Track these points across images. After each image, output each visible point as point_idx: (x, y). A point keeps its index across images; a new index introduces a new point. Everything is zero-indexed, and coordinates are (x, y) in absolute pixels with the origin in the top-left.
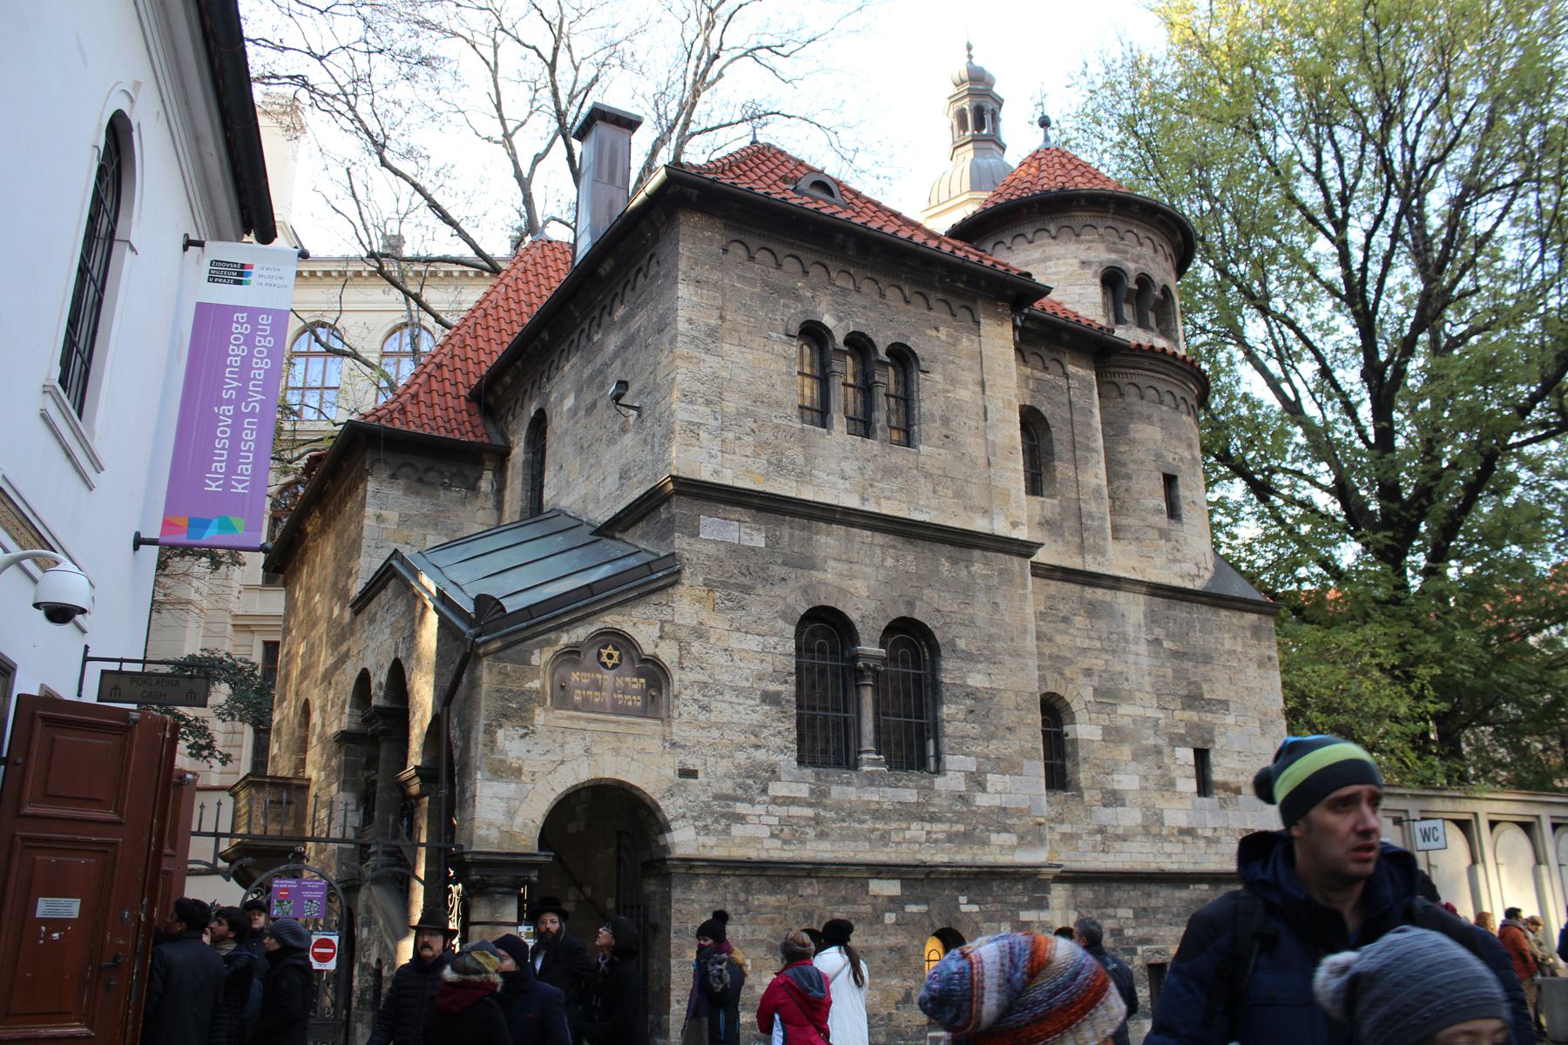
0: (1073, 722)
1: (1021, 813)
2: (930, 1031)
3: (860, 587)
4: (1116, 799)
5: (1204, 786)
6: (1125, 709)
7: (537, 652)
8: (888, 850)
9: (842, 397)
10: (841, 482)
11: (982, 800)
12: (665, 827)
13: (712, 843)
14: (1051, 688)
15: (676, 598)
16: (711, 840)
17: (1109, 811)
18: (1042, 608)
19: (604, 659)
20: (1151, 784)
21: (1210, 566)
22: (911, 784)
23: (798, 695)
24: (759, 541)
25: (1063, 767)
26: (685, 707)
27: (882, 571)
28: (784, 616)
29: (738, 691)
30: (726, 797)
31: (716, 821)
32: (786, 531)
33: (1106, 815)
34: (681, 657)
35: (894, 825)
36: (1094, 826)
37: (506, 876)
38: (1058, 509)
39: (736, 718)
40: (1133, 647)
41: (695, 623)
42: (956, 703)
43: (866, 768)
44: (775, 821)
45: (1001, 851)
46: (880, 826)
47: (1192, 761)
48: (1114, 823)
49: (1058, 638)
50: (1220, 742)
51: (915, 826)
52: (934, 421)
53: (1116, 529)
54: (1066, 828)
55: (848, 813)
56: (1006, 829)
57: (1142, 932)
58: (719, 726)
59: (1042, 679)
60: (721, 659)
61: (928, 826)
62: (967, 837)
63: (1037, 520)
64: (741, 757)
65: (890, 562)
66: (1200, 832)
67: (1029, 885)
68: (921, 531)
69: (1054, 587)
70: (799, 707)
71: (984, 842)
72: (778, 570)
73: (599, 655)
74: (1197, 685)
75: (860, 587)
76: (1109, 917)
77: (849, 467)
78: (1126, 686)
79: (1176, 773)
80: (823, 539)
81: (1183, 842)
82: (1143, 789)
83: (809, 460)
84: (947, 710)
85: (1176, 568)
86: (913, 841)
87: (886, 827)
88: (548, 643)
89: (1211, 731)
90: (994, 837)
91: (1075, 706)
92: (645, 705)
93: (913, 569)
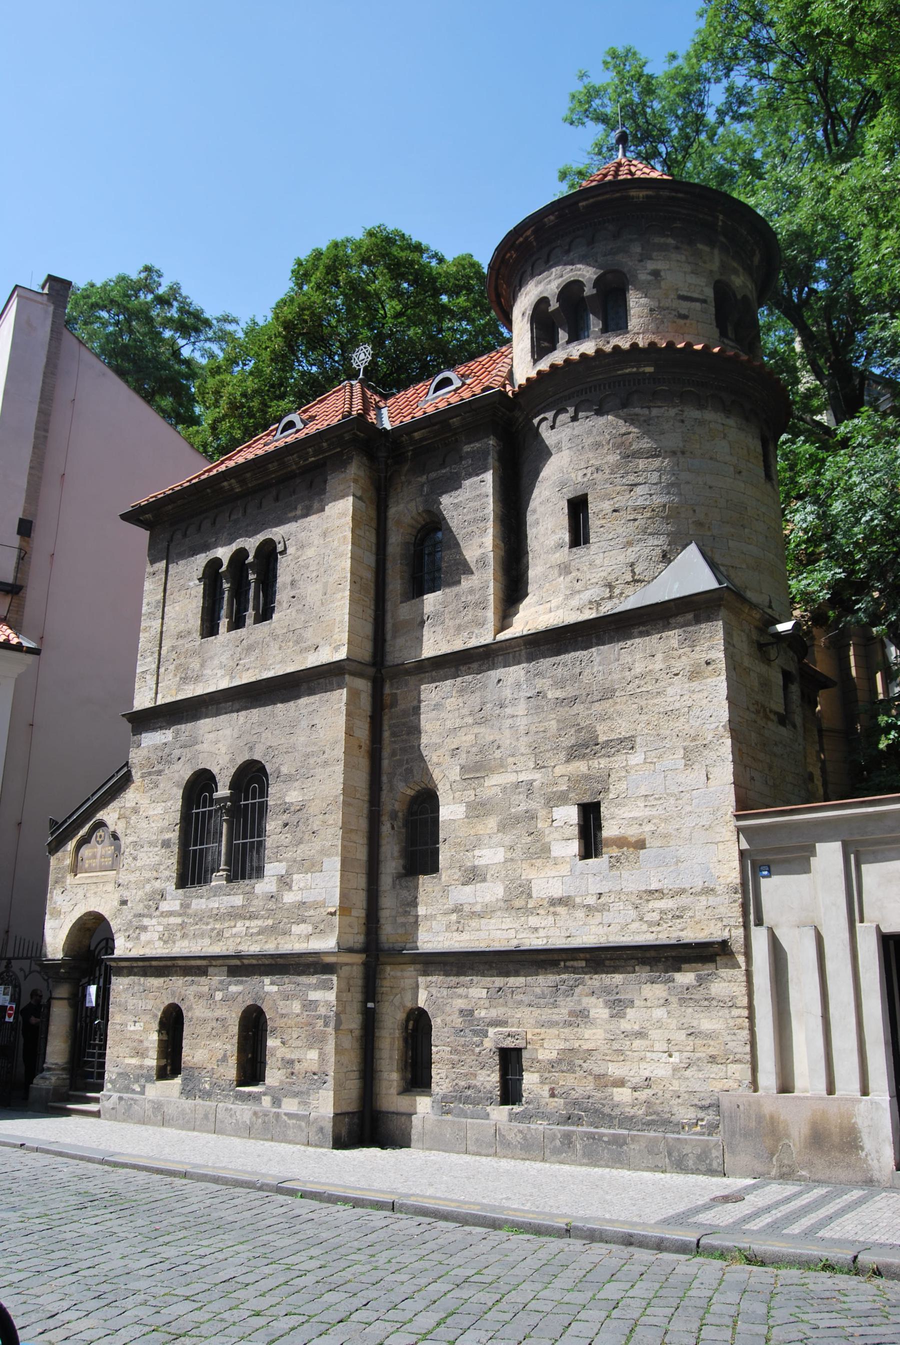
1: (316, 905)
2: (239, 1085)
6: (495, 782)
8: (221, 944)
11: (289, 898)
13: (131, 946)
17: (468, 889)
20: (518, 853)
22: (240, 891)
28: (178, 786)
29: (151, 844)
30: (140, 915)
33: (465, 894)
35: (226, 925)
36: (450, 904)
40: (509, 711)
41: (134, 804)
44: (161, 928)
48: (472, 901)
55: (200, 918)
56: (304, 921)
57: (493, 1013)
58: (140, 869)
61: (247, 923)
64: (148, 888)
66: (578, 900)
76: (460, 996)
78: (498, 754)
81: (555, 914)
83: (202, 666)
85: (575, 602)
86: (235, 936)
87: (222, 927)
89: (604, 781)
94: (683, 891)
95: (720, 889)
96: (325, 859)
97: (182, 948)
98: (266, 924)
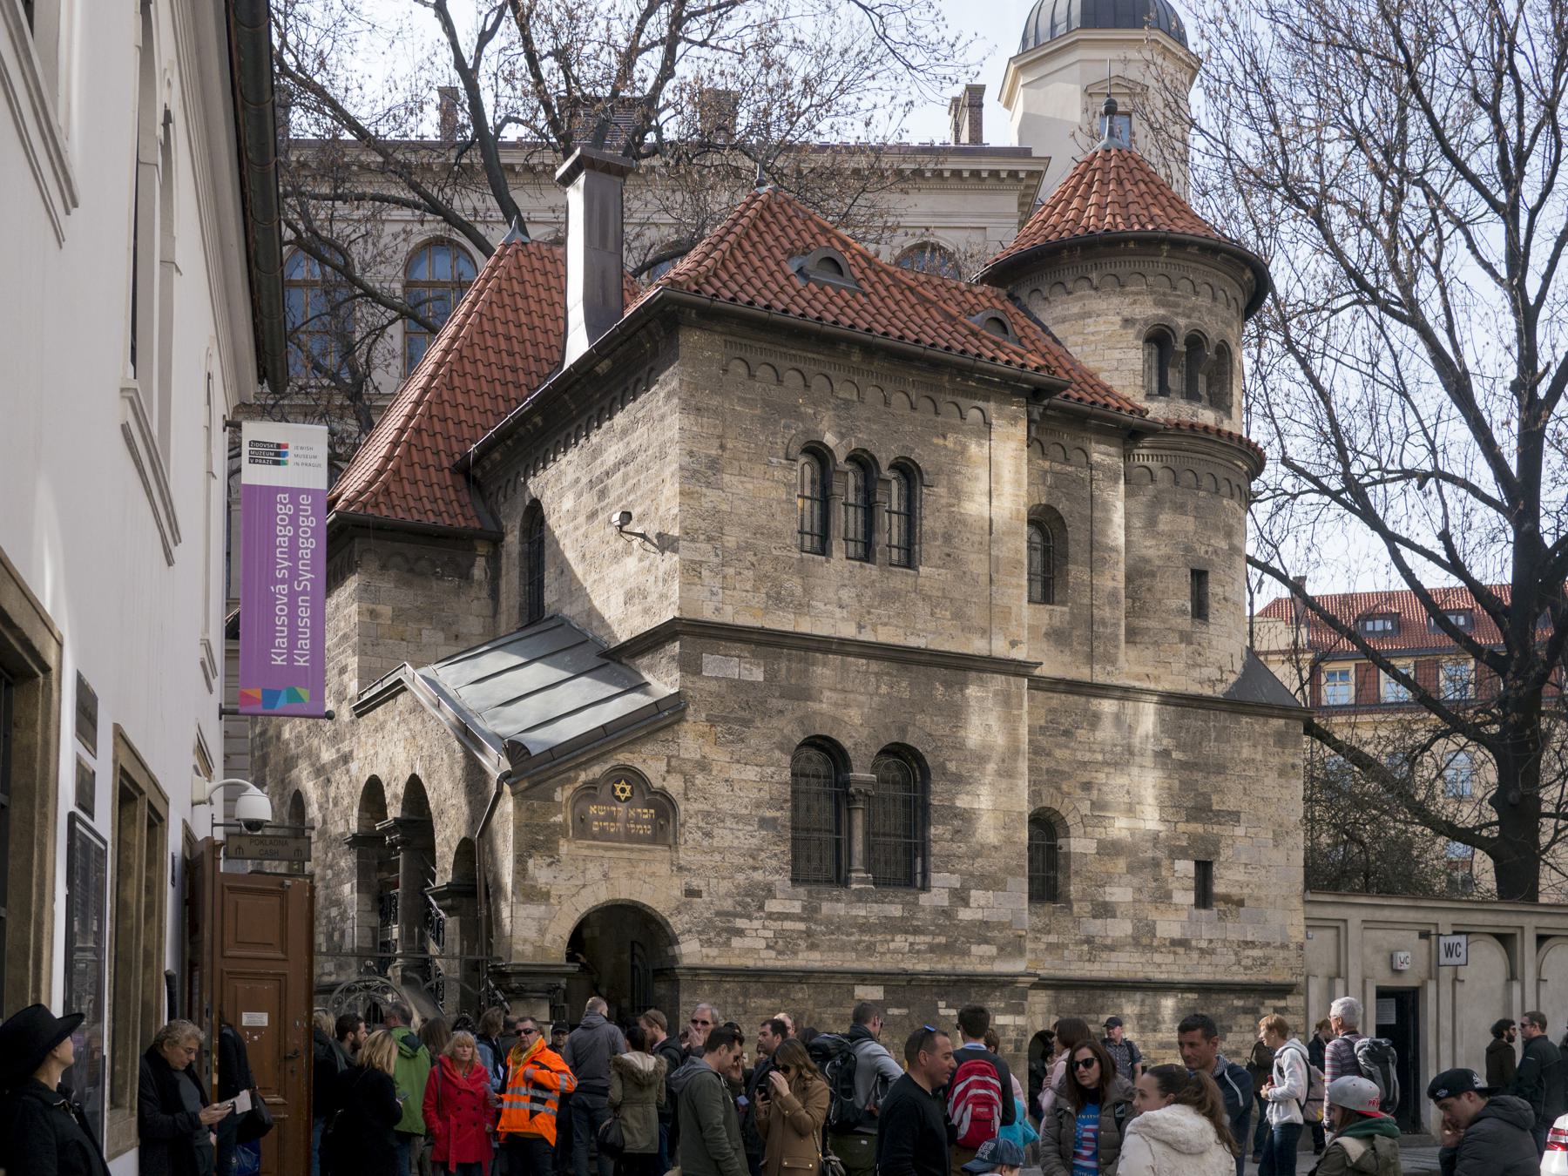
0: (1067, 835)
1: (1001, 926)
3: (854, 715)
4: (1107, 911)
5: (1204, 897)
7: (559, 790)
9: (846, 519)
10: (837, 610)
11: (965, 915)
12: (674, 941)
14: (1047, 803)
15: (681, 734)
16: (713, 952)
17: (1099, 922)
18: (1042, 722)
19: (618, 793)
20: (1145, 896)
21: (1239, 667)
23: (794, 819)
24: (758, 675)
25: (1055, 878)
26: (691, 836)
27: (876, 699)
28: (781, 747)
29: (737, 818)
31: (719, 934)
32: (784, 665)
33: (1095, 927)
34: (686, 789)
35: (879, 937)
37: (540, 983)
38: (1067, 617)
39: (736, 843)
42: (944, 824)
43: (854, 886)
44: (770, 934)
45: (980, 960)
46: (866, 938)
47: (1192, 873)
49: (1058, 753)
50: (1226, 853)
51: (898, 938)
52: (935, 539)
53: (1133, 635)
54: (1052, 938)
55: (837, 927)
56: (986, 941)
58: (721, 851)
59: (1035, 795)
60: (723, 789)
61: (911, 939)
62: (948, 949)
63: (1044, 630)
64: (740, 878)
65: (884, 689)
66: (1194, 943)
67: (1007, 991)
68: (916, 657)
69: (1056, 700)
70: (794, 829)
71: (965, 953)
72: (776, 703)
73: (614, 789)
74: (1207, 797)
75: (854, 715)
77: (846, 595)
79: (1173, 885)
80: (819, 670)
81: (1175, 953)
82: (1134, 901)
83: (807, 590)
84: (933, 830)
85: (1196, 673)
86: (896, 952)
88: (569, 781)
89: (1214, 844)
90: (974, 948)
91: (1070, 820)
92: (654, 834)
93: (906, 695)
94: (1268, 944)
95: (1292, 946)
96: (1009, 879)
97: (807, 959)
98: (937, 940)
